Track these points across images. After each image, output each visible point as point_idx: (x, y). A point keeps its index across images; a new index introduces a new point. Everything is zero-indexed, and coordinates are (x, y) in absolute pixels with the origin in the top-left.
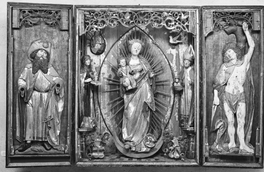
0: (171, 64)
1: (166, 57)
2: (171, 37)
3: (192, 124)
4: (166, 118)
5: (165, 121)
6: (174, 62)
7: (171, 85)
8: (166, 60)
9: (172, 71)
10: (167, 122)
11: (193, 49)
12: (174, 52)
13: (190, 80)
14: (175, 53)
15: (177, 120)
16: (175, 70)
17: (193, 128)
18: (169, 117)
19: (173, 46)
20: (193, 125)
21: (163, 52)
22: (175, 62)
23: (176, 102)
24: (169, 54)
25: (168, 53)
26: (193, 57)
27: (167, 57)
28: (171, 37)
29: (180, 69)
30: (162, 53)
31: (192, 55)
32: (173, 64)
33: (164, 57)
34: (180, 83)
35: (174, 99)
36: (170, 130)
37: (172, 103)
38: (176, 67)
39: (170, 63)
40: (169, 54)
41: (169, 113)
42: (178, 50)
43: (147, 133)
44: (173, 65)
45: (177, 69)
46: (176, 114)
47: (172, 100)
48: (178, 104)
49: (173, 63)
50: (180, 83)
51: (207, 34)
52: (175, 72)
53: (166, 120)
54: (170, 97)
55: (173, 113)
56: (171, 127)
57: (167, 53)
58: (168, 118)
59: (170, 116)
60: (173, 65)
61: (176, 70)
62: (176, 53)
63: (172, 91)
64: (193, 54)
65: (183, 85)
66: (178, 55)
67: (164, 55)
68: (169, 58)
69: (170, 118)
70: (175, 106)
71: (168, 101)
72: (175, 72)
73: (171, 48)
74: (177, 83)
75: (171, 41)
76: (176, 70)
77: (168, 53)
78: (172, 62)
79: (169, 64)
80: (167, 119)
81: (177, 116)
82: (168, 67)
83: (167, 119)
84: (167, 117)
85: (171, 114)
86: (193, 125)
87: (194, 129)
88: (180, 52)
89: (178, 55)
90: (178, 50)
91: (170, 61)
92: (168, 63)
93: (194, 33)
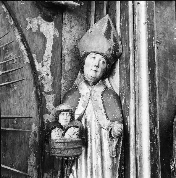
0: (38, 66)
7: (33, 139)
8: (22, 47)
9: (39, 88)
11: (113, 28)
14: (52, 35)
16: (47, 88)
24: (34, 30)
25: (31, 29)
27: (27, 37)
29: (63, 86)
30: (12, 23)
32: (43, 66)
34: (77, 130)
38: (50, 76)
39: (35, 60)
40: (34, 30)
49: (45, 64)
50: (77, 130)
52: (47, 93)
57: (28, 27)
61: (51, 89)
62: (55, 36)
63: (32, 160)
72: (47, 93)
73: (39, 17)
74: (64, 130)
76: (51, 89)
77: (31, 29)
78: (40, 59)
79: (32, 65)
82: (27, 72)
91: (34, 56)
92: (27, 60)
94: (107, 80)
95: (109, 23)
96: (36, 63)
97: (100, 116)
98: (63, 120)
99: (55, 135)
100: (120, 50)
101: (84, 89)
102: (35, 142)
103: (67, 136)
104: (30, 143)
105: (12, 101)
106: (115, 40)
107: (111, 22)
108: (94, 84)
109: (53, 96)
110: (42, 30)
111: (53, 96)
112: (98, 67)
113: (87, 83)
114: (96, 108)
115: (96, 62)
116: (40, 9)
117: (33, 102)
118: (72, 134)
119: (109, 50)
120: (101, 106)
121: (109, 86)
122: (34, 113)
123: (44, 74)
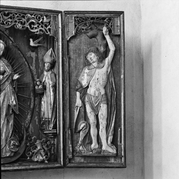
0: (31, 67)
1: (26, 60)
2: (31, 40)
3: (53, 126)
4: (27, 122)
5: (25, 124)
6: (34, 65)
8: (26, 63)
9: (32, 74)
10: (28, 126)
12: (33, 55)
13: (51, 82)
15: (37, 124)
16: (35, 73)
17: (55, 130)
18: (29, 121)
19: (33, 49)
20: (55, 127)
21: (23, 55)
22: (35, 65)
23: (36, 105)
24: (29, 56)
25: (28, 56)
26: (54, 60)
27: (27, 59)
28: (31, 40)
31: (53, 58)
33: (24, 60)
35: (34, 102)
36: (31, 134)
37: (32, 106)
40: (29, 56)
41: (29, 117)
42: (37, 53)
43: (10, 137)
44: (33, 68)
45: (37, 72)
46: (36, 117)
47: (32, 103)
48: (38, 108)
51: (69, 38)
53: (27, 124)
54: (31, 99)
55: (33, 117)
56: (32, 131)
58: (28, 122)
59: (30, 120)
60: (33, 68)
63: (32, 94)
64: (54, 57)
65: (44, 88)
66: (37, 58)
67: (24, 58)
68: (29, 60)
69: (30, 122)
70: (35, 109)
71: (29, 104)
75: (32, 44)
76: (36, 74)
77: (28, 56)
78: (32, 65)
79: (30, 67)
80: (27, 122)
81: (37, 120)
82: (28, 69)
83: (27, 122)
84: (28, 121)
85: (31, 117)
86: (55, 127)
87: (57, 131)
88: (40, 55)
89: (37, 58)
90: (37, 53)
92: (28, 66)
93: (56, 36)
94: (52, 69)
95: (52, 51)
96: (31, 67)
97: (49, 81)
98: (38, 83)
99: (36, 87)
100: (55, 60)
101: (45, 73)
102: (32, 89)
103: (39, 88)
104: (31, 90)
105: (25, 79)
106: (54, 57)
107: (52, 50)
108: (48, 71)
109: (36, 75)
110: (31, 56)
111: (36, 75)
112: (48, 67)
113: (46, 71)
114: (48, 79)
115: (47, 65)
116: (30, 49)
117: (31, 78)
118: (40, 87)
119: (51, 61)
120: (50, 78)
121: (53, 71)
122: (31, 81)
123: (33, 69)
